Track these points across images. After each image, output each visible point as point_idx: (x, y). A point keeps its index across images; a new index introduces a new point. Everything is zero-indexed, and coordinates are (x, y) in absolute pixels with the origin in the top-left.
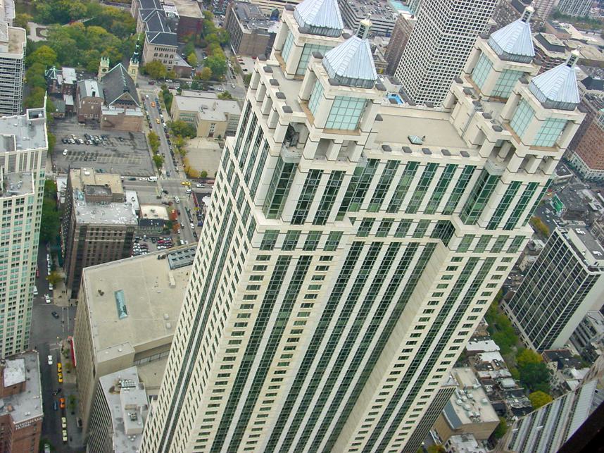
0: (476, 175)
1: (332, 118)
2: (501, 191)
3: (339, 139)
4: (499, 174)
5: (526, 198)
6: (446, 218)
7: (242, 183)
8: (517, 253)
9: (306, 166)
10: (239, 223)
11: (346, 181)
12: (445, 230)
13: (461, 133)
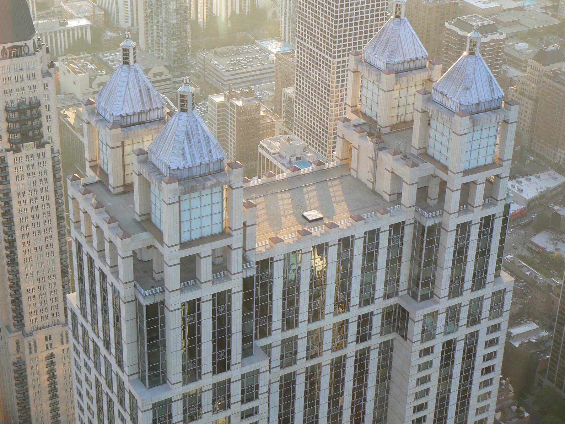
1: (185, 226)
2: (449, 241)
4: (437, 221)
6: (392, 302)
7: (103, 351)
8: (504, 314)
9: (175, 301)
10: (117, 406)
12: (397, 319)
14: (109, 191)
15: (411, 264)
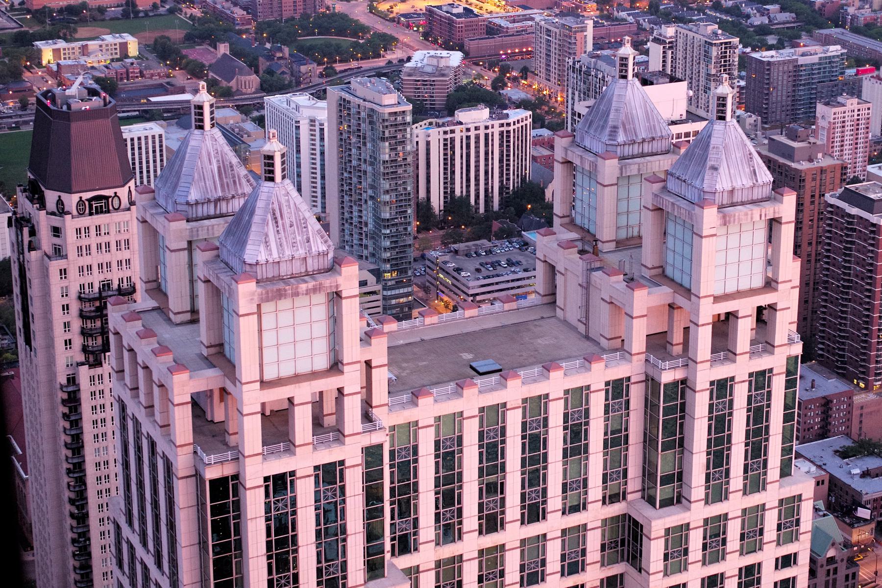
0: (636, 395)
1: (269, 355)
3: (303, 393)
5: (759, 410)
6: (616, 509)
8: (802, 537)
11: (354, 483)
12: (626, 540)
13: (582, 328)
14: (170, 319)
15: (644, 448)
